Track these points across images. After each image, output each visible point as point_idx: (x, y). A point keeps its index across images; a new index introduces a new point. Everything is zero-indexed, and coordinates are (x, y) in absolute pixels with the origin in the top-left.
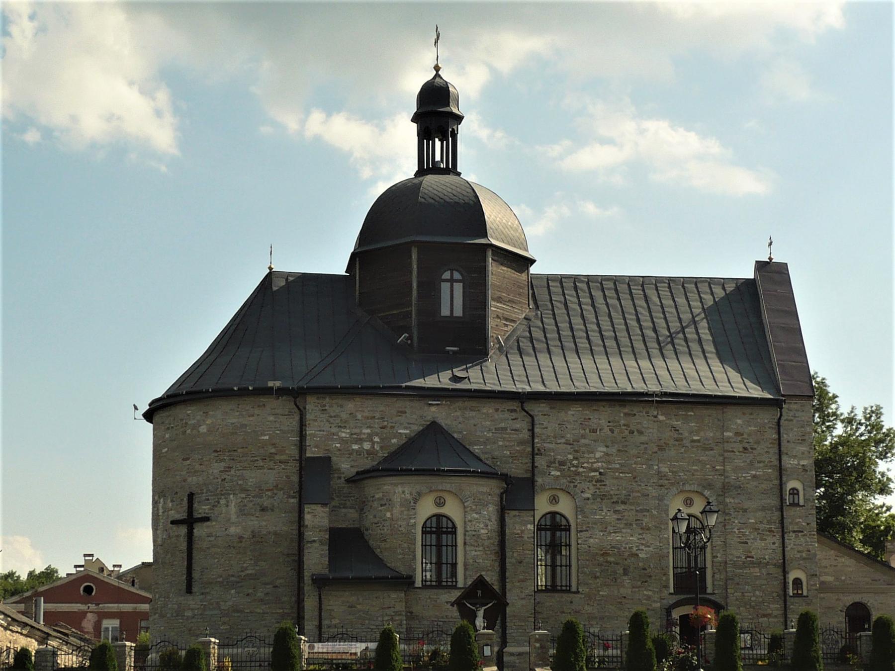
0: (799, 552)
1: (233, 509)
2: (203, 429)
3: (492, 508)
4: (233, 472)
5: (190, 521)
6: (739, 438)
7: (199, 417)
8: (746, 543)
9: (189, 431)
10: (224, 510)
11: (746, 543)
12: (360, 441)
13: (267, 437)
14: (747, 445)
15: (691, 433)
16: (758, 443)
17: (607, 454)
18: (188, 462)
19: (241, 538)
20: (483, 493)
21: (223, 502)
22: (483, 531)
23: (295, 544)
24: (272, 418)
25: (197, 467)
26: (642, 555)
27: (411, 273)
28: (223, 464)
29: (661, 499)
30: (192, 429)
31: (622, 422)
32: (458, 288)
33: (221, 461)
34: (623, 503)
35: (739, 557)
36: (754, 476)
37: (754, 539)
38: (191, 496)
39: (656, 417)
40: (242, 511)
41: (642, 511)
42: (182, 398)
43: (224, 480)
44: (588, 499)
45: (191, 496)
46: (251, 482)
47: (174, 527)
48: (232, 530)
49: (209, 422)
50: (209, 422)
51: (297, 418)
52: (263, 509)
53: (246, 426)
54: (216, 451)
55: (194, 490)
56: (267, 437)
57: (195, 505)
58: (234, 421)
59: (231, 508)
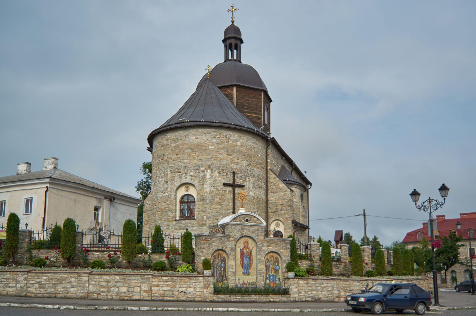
1: (251, 185)
2: (239, 143)
4: (251, 167)
5: (234, 186)
7: (236, 137)
9: (231, 142)
10: (248, 183)
12: (275, 166)
13: (260, 155)
18: (231, 157)
19: (254, 198)
21: (248, 180)
23: (265, 205)
24: (261, 147)
25: (236, 160)
27: (261, 102)
28: (247, 163)
30: (233, 142)
33: (247, 161)
38: (234, 173)
40: (254, 187)
42: (231, 126)
43: (248, 170)
45: (234, 173)
46: (256, 173)
47: (222, 187)
48: (251, 194)
49: (241, 141)
50: (241, 141)
51: (265, 150)
52: (259, 187)
53: (254, 147)
54: (244, 155)
55: (235, 171)
56: (260, 155)
57: (236, 178)
58: (251, 144)
59: (249, 183)
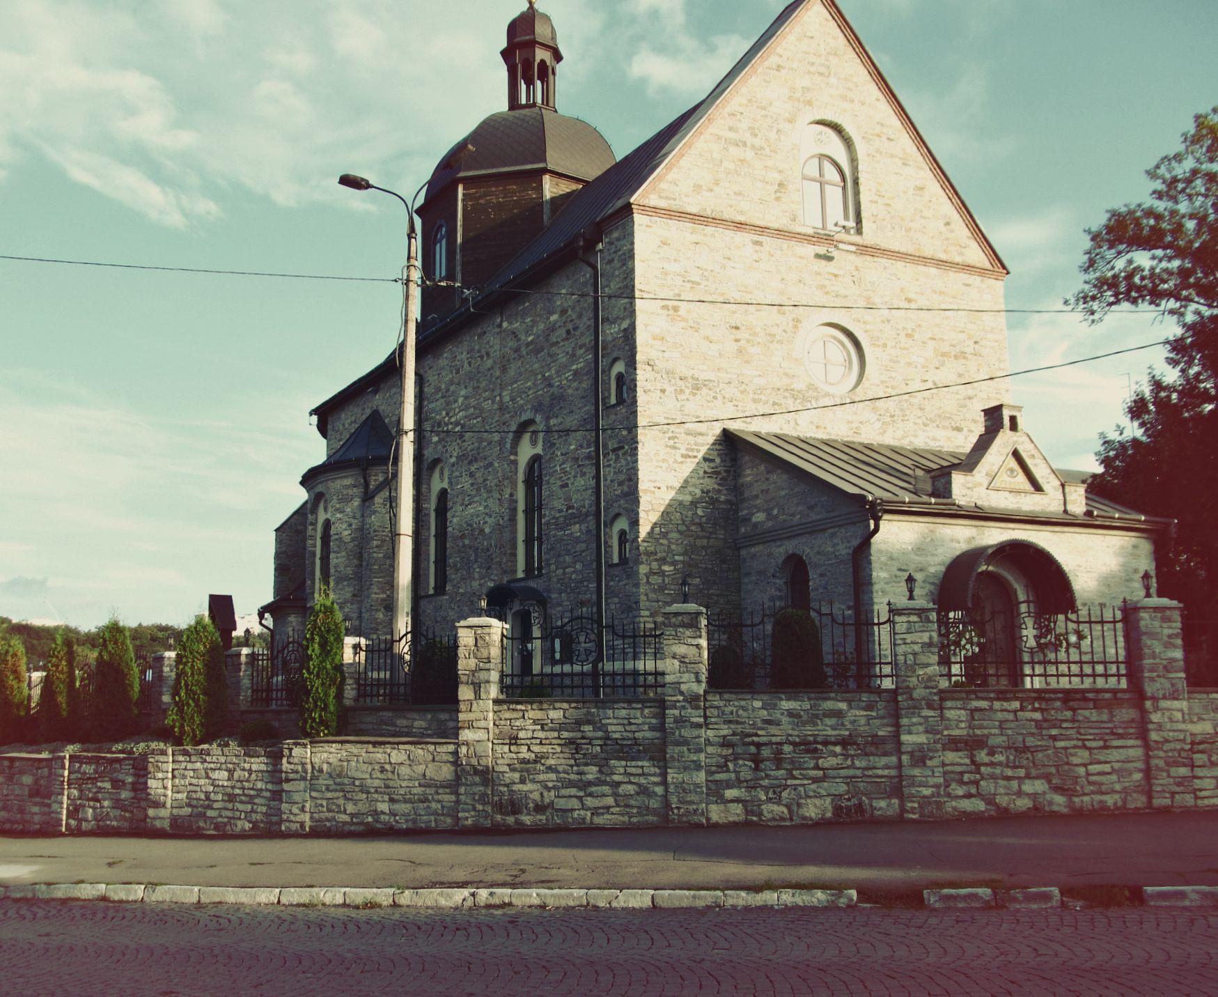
0: (621, 484)
3: (356, 503)
6: (564, 319)
8: (566, 485)
11: (566, 485)
14: (570, 326)
15: (527, 333)
16: (580, 316)
17: (466, 398)
20: (347, 487)
22: (347, 533)
26: (487, 530)
29: (501, 443)
31: (477, 347)
32: (444, 242)
34: (476, 460)
35: (561, 511)
36: (576, 373)
37: (575, 477)
39: (500, 326)
41: (486, 467)
44: (453, 465)
